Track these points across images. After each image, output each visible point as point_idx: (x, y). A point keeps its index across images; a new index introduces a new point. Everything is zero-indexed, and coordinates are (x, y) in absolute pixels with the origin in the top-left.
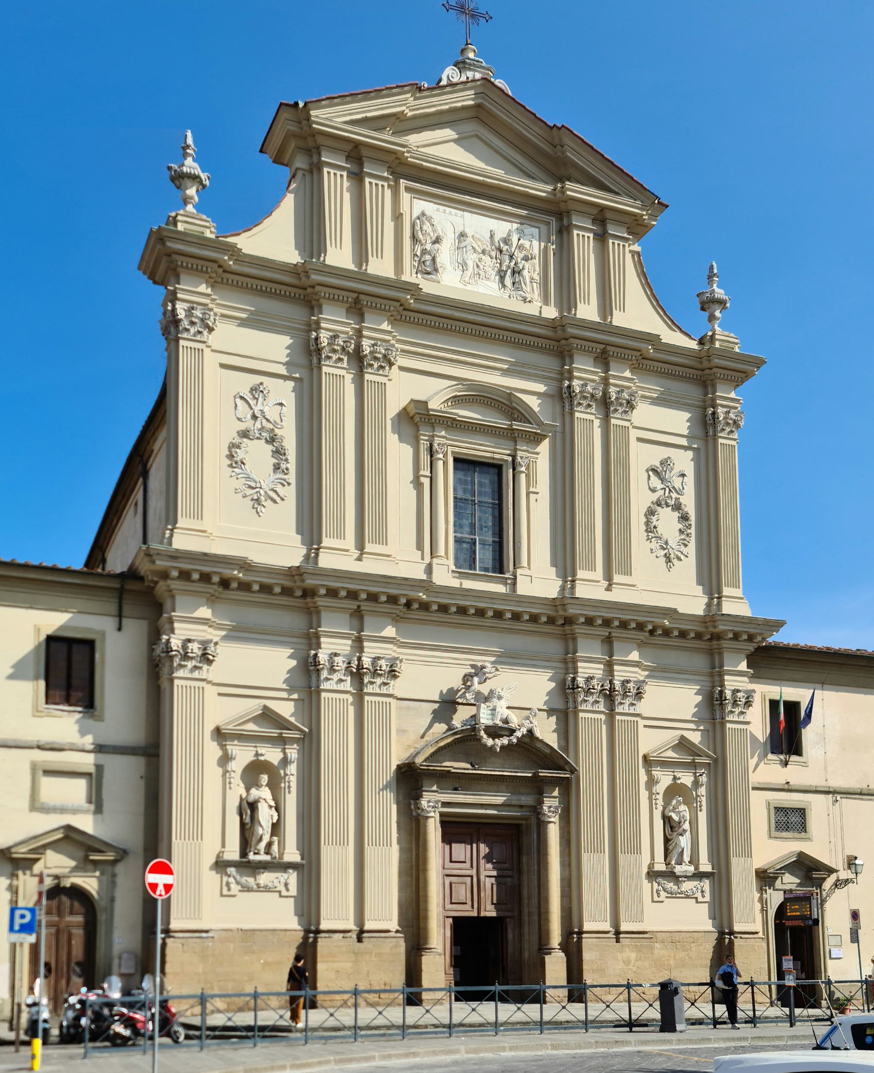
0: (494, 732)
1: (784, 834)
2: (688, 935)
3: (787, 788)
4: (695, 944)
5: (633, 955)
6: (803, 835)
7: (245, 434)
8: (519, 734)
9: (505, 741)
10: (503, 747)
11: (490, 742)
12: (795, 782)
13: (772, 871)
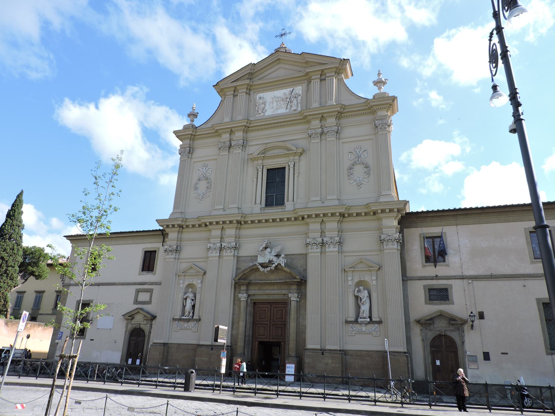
2: (366, 353)
3: (437, 277)
4: (369, 357)
5: (330, 361)
6: (447, 302)
7: (199, 180)
8: (274, 265)
12: (439, 274)
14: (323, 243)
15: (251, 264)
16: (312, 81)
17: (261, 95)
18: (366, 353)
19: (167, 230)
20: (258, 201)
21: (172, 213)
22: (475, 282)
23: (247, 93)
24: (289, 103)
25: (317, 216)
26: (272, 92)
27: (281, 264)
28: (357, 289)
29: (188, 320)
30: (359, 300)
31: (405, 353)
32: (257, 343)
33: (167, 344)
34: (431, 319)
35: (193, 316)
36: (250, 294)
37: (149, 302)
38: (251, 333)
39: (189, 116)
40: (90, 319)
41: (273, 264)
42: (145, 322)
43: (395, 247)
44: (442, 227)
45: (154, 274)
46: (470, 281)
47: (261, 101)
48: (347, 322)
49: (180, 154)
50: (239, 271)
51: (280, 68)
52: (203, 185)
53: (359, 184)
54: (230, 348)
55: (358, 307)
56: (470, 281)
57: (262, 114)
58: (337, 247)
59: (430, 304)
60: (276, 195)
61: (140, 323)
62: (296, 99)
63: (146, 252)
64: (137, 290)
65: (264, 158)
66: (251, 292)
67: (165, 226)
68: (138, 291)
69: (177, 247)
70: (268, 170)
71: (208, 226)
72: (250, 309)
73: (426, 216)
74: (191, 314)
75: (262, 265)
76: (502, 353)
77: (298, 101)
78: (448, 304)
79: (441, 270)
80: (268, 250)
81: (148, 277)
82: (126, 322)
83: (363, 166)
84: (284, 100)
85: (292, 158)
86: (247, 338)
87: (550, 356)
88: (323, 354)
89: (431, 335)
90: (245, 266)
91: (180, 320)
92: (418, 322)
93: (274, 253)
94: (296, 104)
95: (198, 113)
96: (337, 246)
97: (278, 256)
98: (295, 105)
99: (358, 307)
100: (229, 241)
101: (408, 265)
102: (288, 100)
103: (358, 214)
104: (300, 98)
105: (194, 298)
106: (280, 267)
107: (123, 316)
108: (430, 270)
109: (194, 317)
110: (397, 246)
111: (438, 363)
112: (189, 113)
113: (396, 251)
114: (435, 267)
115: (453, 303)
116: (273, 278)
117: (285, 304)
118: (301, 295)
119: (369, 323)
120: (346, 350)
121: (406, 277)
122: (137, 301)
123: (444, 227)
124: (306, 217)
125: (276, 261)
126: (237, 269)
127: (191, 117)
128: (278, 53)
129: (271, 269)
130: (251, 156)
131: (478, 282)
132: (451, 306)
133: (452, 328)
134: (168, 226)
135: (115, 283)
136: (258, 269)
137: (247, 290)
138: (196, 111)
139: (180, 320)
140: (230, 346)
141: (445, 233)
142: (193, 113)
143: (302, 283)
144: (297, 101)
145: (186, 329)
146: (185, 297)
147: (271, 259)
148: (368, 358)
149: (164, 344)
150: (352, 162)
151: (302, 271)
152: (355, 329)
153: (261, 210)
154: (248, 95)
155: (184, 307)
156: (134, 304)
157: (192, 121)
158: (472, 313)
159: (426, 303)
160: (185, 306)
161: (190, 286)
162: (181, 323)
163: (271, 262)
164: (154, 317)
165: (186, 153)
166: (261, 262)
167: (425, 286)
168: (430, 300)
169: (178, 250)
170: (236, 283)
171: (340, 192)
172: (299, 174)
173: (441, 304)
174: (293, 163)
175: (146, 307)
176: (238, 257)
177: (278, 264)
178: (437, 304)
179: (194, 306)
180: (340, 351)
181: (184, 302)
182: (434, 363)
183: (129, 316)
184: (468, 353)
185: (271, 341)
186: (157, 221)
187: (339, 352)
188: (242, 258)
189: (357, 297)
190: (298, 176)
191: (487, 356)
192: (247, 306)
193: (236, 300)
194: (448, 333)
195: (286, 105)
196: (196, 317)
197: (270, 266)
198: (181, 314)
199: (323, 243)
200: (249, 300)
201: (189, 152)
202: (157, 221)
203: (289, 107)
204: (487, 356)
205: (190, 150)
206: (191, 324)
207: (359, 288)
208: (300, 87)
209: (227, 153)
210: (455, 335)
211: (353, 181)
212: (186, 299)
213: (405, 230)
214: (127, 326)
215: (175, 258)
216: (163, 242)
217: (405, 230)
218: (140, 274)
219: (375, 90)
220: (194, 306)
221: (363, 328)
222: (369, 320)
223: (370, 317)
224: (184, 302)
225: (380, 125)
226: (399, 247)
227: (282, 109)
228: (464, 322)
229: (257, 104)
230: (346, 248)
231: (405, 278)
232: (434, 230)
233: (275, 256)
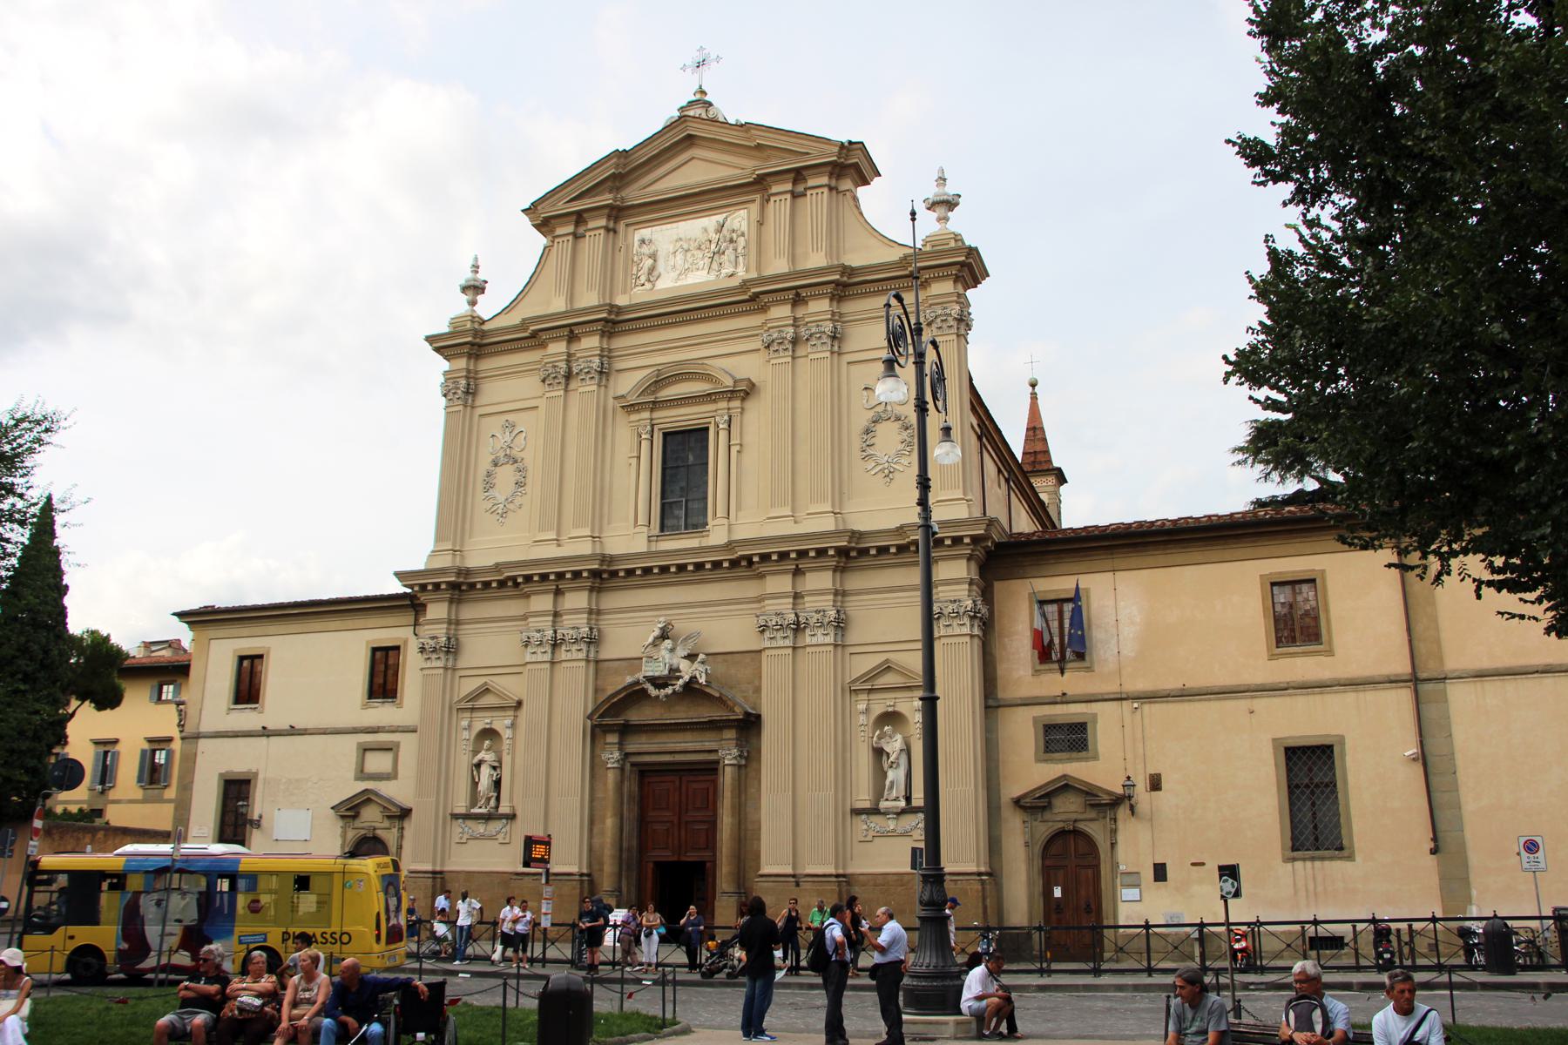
0: (659, 682)
1: (1057, 755)
3: (1064, 699)
6: (1083, 754)
8: (681, 682)
9: (669, 690)
10: (666, 696)
11: (653, 692)
13: (1028, 800)
14: (797, 623)
15: (629, 679)
16: (772, 199)
17: (645, 233)
18: (895, 877)
19: (423, 598)
20: (642, 519)
21: (433, 551)
22: (1146, 707)
23: (607, 229)
24: (716, 257)
25: (784, 556)
26: (674, 225)
27: (698, 676)
28: (878, 733)
29: (488, 818)
30: (885, 758)
31: (980, 874)
32: (651, 865)
33: (441, 872)
34: (1048, 795)
35: (497, 807)
36: (628, 751)
37: (392, 776)
38: (635, 843)
39: (465, 289)
40: (256, 817)
41: (678, 678)
42: (386, 823)
43: (966, 630)
44: (1076, 577)
45: (400, 706)
46: (1136, 705)
47: (646, 250)
48: (857, 812)
49: (445, 395)
50: (602, 698)
51: (693, 158)
52: (506, 475)
53: (887, 471)
54: (586, 878)
55: (880, 774)
56: (1136, 705)
57: (648, 286)
58: (832, 634)
59: (1045, 761)
60: (687, 502)
61: (373, 824)
62: (731, 245)
63: (375, 650)
64: (359, 744)
65: (655, 405)
66: (631, 748)
67: (416, 588)
68: (365, 750)
69: (449, 639)
70: (666, 435)
71: (522, 586)
72: (631, 786)
73: (1044, 549)
74: (493, 803)
75: (653, 680)
76: (1193, 864)
77: (739, 251)
78: (1086, 759)
79: (1073, 681)
80: (668, 643)
81: (382, 713)
82: (340, 823)
83: (898, 424)
84: (703, 247)
85: (723, 405)
86: (624, 856)
87: (1289, 865)
88: (798, 884)
89: (1044, 830)
90: (618, 682)
91: (467, 817)
92: (1017, 802)
93: (681, 652)
94: (733, 258)
95: (486, 282)
96: (831, 631)
97: (691, 657)
98: (730, 261)
99: (880, 774)
100: (575, 624)
101: (1001, 670)
102: (713, 246)
103: (883, 550)
104: (742, 242)
105: (496, 764)
106: (697, 686)
107: (332, 808)
108: (1053, 683)
109: (502, 810)
110: (972, 626)
111: (1058, 893)
112: (463, 282)
113: (967, 639)
114: (1062, 673)
115: (1095, 758)
116: (682, 714)
117: (711, 769)
118: (748, 752)
119: (903, 812)
120: (852, 875)
121: (996, 699)
122: (362, 771)
123: (1081, 577)
124: (756, 559)
125: (687, 670)
126: (596, 690)
127: (470, 292)
128: (685, 121)
129: (674, 690)
130: (622, 400)
131: (1152, 705)
132: (1091, 763)
133: (1092, 814)
134: (423, 587)
135: (306, 730)
136: (644, 691)
137: (621, 744)
138: (481, 276)
139: (467, 817)
140: (589, 875)
141: (1087, 590)
142: (472, 283)
143: (749, 725)
144: (736, 250)
145: (482, 837)
146: (476, 760)
147: (675, 666)
148: (900, 889)
149: (434, 872)
150: (871, 413)
151: (751, 692)
152: (872, 825)
153: (649, 541)
154: (611, 233)
155: (475, 784)
156: (357, 779)
157: (473, 303)
158: (1129, 778)
159: (1038, 760)
160: (477, 783)
161: (489, 733)
162: (470, 823)
163: (674, 672)
164: (405, 813)
165: (459, 392)
166: (651, 674)
167: (1035, 720)
168: (1048, 750)
169: (452, 648)
170: (594, 727)
171: (841, 493)
172: (741, 445)
173: (1070, 760)
174: (726, 418)
175: (385, 788)
176: (597, 662)
177: (691, 678)
178: (1060, 761)
179: (497, 784)
180: (837, 876)
181: (475, 773)
182: (1047, 892)
183: (347, 810)
184: (1122, 868)
185: (684, 859)
186: (397, 574)
187: (834, 879)
188: (607, 663)
189: (879, 753)
190: (738, 452)
191: (1160, 872)
192: (622, 781)
193: (595, 767)
194: (1081, 826)
195: (707, 261)
196: (504, 809)
197: (674, 682)
198: (468, 804)
199: (797, 623)
200: (628, 766)
201: (468, 389)
202: (397, 574)
203: (715, 266)
204: (1160, 872)
205: (469, 385)
206: (494, 826)
207: (882, 730)
208: (743, 213)
209: (562, 393)
210: (1095, 830)
211: (874, 464)
212: (478, 765)
213: (997, 585)
214: (344, 835)
215: (446, 668)
216: (415, 625)
217: (997, 585)
218: (365, 707)
219: (928, 225)
220: (497, 784)
221: (890, 822)
222: (903, 804)
223: (908, 799)
224: (475, 773)
225: (939, 320)
226: (976, 631)
227: (699, 273)
228: (1117, 801)
229: (635, 259)
230: (853, 636)
231: (991, 702)
232: (1059, 584)
233: (685, 657)
